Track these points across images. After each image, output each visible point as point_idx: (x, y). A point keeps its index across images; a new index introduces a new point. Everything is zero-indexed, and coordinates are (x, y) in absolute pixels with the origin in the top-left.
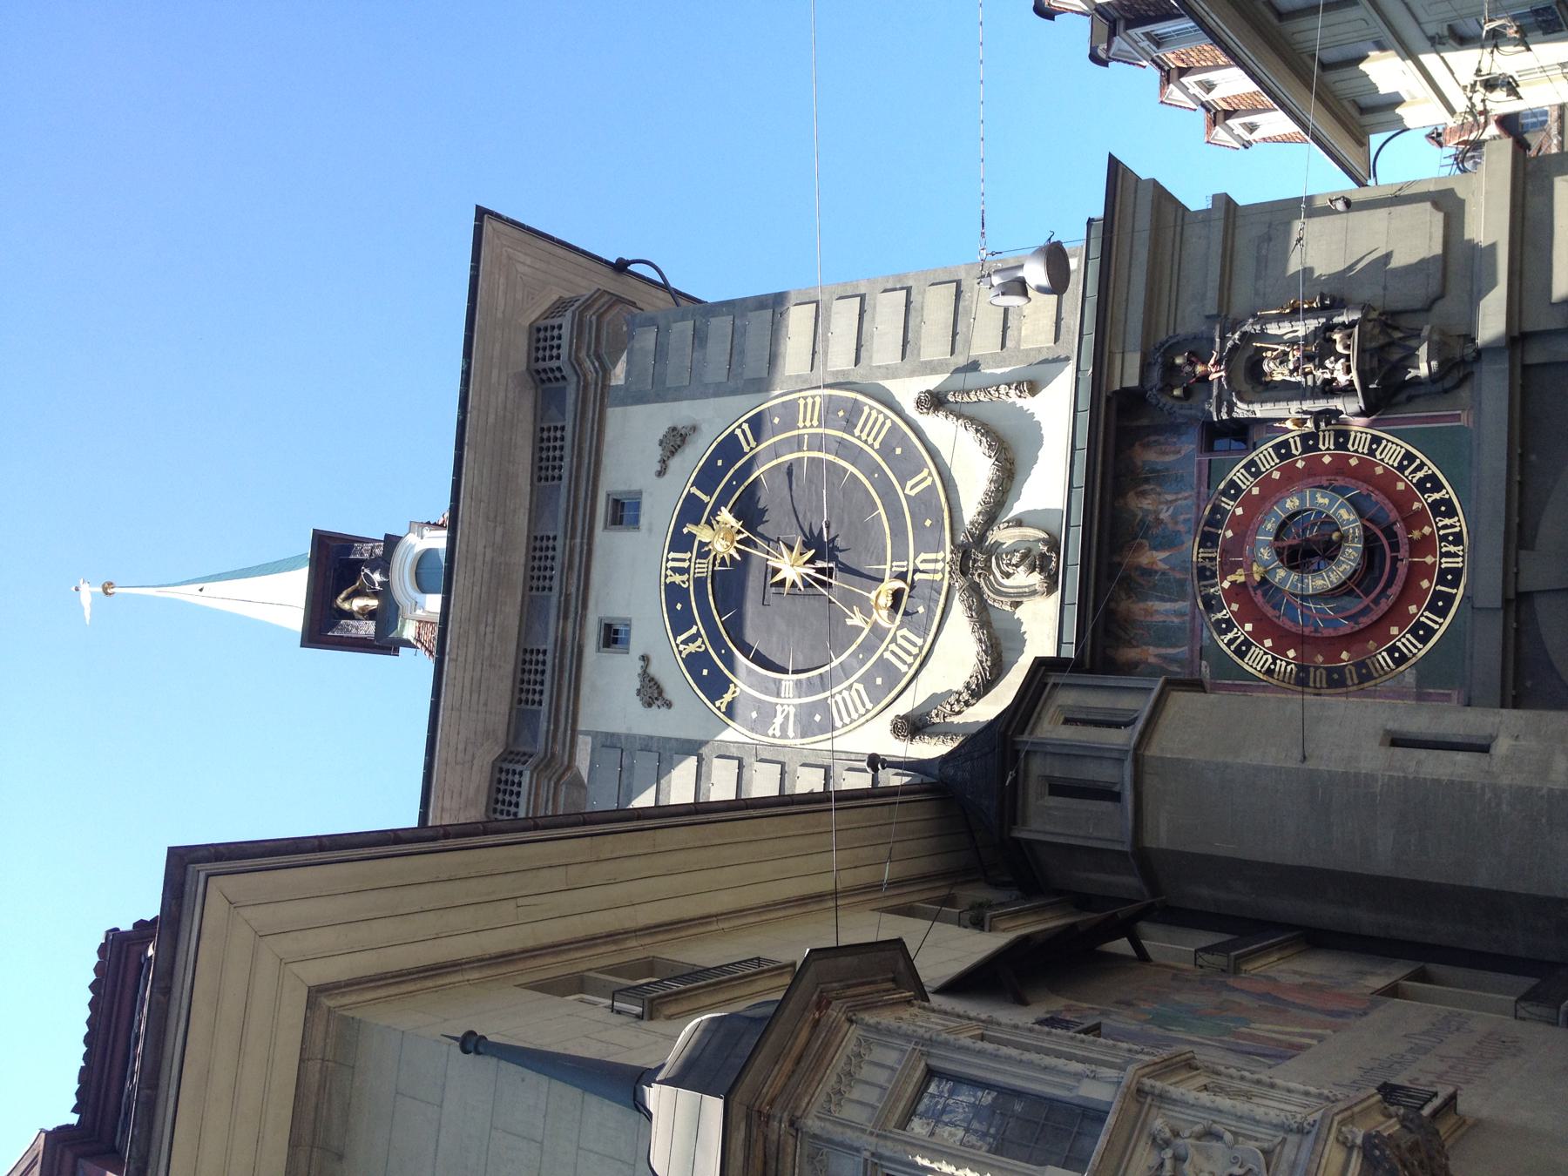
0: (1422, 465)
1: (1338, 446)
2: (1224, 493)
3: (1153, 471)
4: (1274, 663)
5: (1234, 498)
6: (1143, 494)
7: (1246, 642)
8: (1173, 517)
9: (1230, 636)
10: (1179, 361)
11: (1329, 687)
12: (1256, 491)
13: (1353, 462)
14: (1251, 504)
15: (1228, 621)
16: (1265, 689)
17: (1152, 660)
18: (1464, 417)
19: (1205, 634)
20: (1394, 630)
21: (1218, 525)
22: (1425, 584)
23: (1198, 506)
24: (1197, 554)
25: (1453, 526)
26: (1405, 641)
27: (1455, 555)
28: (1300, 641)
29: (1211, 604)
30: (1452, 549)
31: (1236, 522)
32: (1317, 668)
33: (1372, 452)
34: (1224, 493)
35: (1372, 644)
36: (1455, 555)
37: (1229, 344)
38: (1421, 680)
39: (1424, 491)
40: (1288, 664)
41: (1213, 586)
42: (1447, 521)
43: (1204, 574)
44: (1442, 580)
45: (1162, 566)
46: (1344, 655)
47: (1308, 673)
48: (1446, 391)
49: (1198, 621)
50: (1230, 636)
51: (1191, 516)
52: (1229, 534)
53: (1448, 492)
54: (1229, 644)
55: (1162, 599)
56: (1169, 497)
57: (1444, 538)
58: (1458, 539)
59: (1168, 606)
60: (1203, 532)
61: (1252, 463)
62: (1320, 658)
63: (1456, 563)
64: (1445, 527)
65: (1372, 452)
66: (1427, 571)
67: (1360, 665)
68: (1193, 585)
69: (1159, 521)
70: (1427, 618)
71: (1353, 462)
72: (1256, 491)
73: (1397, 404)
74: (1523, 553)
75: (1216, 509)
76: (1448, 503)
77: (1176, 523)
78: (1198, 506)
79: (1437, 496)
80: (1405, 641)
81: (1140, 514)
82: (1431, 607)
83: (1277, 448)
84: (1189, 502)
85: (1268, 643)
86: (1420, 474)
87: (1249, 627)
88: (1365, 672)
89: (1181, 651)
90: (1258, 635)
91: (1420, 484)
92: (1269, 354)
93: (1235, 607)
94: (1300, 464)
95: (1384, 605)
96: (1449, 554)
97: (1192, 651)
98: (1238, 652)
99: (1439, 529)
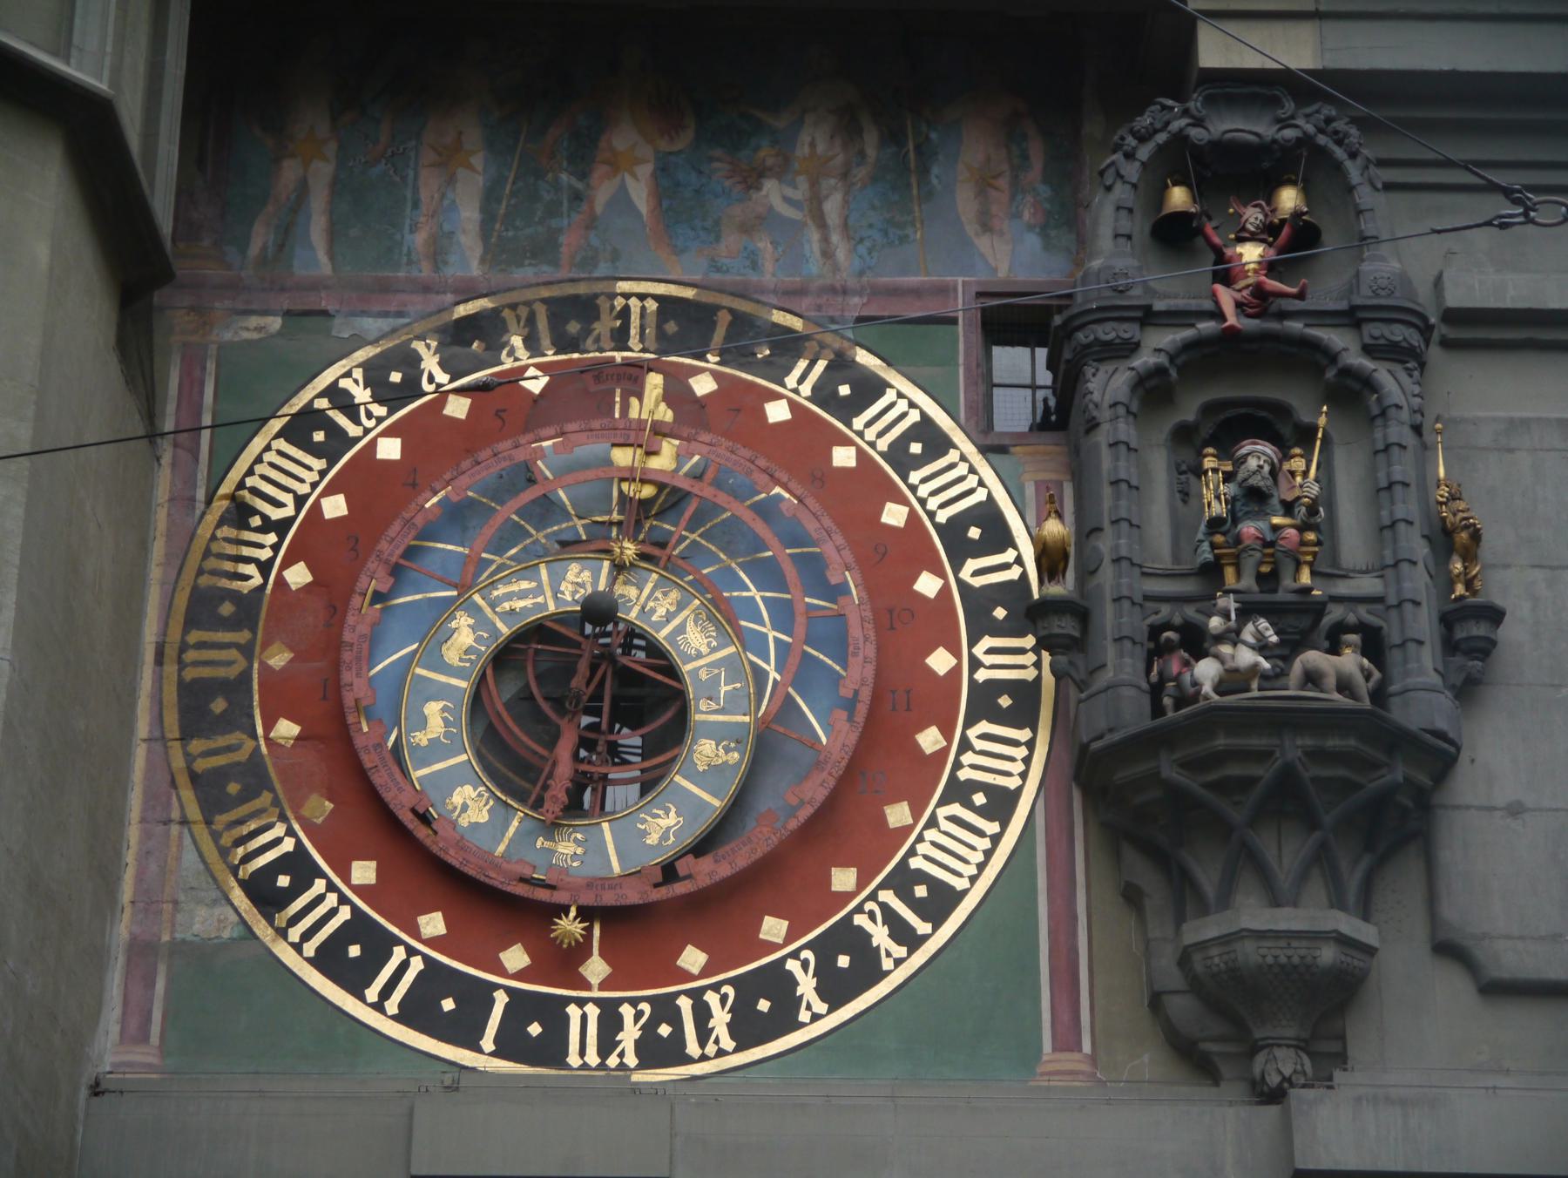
0: (912, 941)
1: (984, 702)
2: (841, 366)
3: (925, 155)
4: (268, 526)
5: (823, 394)
6: (849, 128)
7: (339, 440)
8: (765, 220)
9: (362, 395)
10: (1289, 199)
11: (184, 688)
12: (843, 457)
13: (929, 739)
14: (804, 442)
15: (411, 389)
17: (290, 172)
18: (1069, 1061)
19: (371, 325)
20: (364, 872)
21: (735, 354)
22: (515, 958)
23: (801, 292)
24: (638, 293)
25: (704, 1035)
26: (328, 904)
27: (607, 1044)
29: (465, 338)
30: (630, 1034)
31: (738, 406)
32: (247, 650)
33: (959, 792)
34: (841, 366)
35: (321, 808)
36: (607, 1044)
37: (1336, 338)
38: (197, 958)
39: (825, 949)
40: (264, 568)
41: (532, 345)
42: (720, 1019)
43: (572, 317)
44: (522, 1008)
45: (602, 194)
46: (287, 729)
47: (232, 624)
48: (1156, 1002)
49: (416, 304)
50: (362, 395)
51: (770, 274)
52: (703, 385)
53: (818, 1020)
54: (332, 392)
55: (489, 199)
56: (832, 207)
58: (655, 1051)
59: (469, 214)
60: (713, 309)
61: (937, 444)
62: (279, 659)
63: (581, 1051)
64: (702, 1014)
66: (562, 963)
67: (254, 776)
68: (534, 281)
69: (752, 178)
70: (404, 966)
72: (843, 457)
73: (1117, 856)
75: (788, 347)
76: (785, 1020)
77: (746, 229)
78: (801, 292)
79: (806, 985)
80: (328, 904)
81: (781, 123)
82: (434, 976)
83: (987, 514)
84: (814, 266)
85: (335, 507)
86: (880, 935)
88: (224, 793)
89: (316, 256)
90: (363, 479)
93: (458, 408)
94: (927, 585)
96: (610, 1024)
97: (315, 286)
99: (696, 995)
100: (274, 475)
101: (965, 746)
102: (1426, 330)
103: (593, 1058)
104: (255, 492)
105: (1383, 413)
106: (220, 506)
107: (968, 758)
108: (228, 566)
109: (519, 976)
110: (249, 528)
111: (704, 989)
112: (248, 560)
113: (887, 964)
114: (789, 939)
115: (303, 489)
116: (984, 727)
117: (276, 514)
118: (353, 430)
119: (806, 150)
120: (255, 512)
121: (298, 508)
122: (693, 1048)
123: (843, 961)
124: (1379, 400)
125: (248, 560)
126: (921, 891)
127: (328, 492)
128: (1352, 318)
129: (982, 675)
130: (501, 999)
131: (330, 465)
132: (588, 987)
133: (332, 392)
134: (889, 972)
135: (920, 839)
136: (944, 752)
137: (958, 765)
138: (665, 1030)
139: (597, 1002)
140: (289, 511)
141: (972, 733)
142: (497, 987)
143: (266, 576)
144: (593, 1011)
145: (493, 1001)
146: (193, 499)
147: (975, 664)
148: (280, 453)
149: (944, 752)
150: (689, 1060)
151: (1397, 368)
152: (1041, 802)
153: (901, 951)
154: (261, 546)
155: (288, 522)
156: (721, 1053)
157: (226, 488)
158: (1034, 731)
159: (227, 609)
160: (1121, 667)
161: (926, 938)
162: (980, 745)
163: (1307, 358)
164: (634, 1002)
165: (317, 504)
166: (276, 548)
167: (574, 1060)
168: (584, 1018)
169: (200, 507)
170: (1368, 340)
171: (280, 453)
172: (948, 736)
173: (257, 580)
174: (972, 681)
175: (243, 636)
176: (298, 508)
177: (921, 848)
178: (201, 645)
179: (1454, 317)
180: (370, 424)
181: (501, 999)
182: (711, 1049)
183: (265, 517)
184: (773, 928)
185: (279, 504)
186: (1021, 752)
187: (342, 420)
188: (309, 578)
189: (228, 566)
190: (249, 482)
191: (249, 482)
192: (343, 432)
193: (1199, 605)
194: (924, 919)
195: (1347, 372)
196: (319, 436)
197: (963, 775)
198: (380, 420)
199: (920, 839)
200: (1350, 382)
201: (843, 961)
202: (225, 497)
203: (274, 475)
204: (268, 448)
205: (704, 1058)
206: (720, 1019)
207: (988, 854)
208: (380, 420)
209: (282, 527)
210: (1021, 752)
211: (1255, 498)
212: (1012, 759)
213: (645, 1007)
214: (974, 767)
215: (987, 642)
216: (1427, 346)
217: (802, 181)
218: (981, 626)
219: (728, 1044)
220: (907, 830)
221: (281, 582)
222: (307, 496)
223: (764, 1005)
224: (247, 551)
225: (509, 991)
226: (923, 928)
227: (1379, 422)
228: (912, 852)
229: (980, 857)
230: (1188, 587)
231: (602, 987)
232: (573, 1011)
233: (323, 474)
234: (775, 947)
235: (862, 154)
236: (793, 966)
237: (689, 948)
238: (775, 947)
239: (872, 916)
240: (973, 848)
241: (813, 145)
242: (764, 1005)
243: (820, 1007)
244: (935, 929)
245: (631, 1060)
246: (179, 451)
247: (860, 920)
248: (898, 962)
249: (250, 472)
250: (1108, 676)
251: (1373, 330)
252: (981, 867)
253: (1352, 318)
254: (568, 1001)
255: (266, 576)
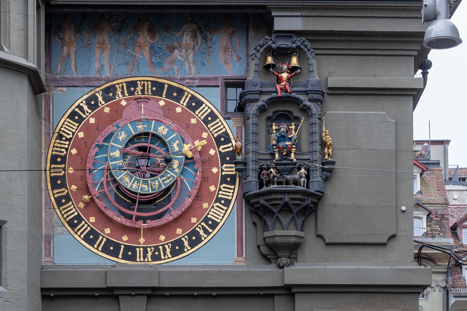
1: (224, 180)
4: (67, 140)
7: (81, 119)
16: (48, 134)
27: (145, 257)
28: (83, 156)
30: (149, 254)
33: (218, 200)
36: (145, 257)
37: (302, 97)
40: (67, 149)
42: (168, 251)
44: (127, 248)
57: (157, 249)
58: (156, 258)
64: (164, 250)
65: (218, 200)
71: (212, 188)
74: (146, 297)
79: (186, 243)
85: (81, 135)
86: (201, 232)
87: (92, 121)
90: (87, 128)
91: (194, 232)
92: (293, 127)
95: (110, 213)
96: (145, 252)
98: (74, 114)
99: (163, 246)
100: (67, 127)
101: (220, 190)
102: (323, 94)
103: (142, 260)
104: (63, 131)
105: (312, 115)
106: (56, 135)
107: (220, 192)
108: (59, 149)
109: (126, 242)
110: (62, 140)
111: (164, 244)
112: (63, 148)
113: (203, 238)
114: (182, 233)
115: (74, 131)
116: (224, 185)
117: (68, 137)
118: (84, 116)
119: (185, 42)
120: (64, 136)
121: (73, 136)
122: (163, 257)
123: (194, 238)
124: (311, 112)
125: (63, 148)
126: (210, 222)
127: (79, 131)
128: (306, 93)
129: (224, 173)
130: (123, 247)
131: (80, 124)
132: (141, 244)
133: (79, 107)
134: (203, 240)
135: (210, 211)
136: (215, 191)
137: (218, 194)
138: (157, 253)
139: (142, 247)
140: (71, 136)
141: (221, 187)
142: (122, 244)
143: (67, 152)
144: (142, 249)
145: (121, 247)
146: (50, 133)
147: (222, 171)
148: (68, 122)
149: (216, 191)
150: (162, 260)
151: (316, 104)
152: (236, 202)
153: (206, 236)
154: (66, 145)
155: (71, 138)
156: (169, 258)
157: (57, 131)
158: (235, 186)
159: (59, 160)
160: (252, 177)
161: (211, 233)
162: (223, 189)
163: (296, 102)
164: (150, 247)
165: (77, 134)
166: (69, 145)
167: (138, 260)
168: (140, 251)
169: (52, 135)
170: (310, 98)
171: (68, 122)
172: (216, 187)
173: (65, 152)
174: (221, 174)
175: (63, 166)
176: (73, 136)
177: (210, 213)
178: (54, 168)
179: (330, 89)
180: (88, 114)
181: (123, 247)
182: (166, 257)
183: (66, 138)
184: (179, 231)
185: (69, 134)
186: (232, 191)
187: (82, 114)
188: (76, 152)
189: (59, 149)
190: (62, 129)
191: (62, 129)
192: (82, 116)
193: (270, 161)
194: (211, 229)
195: (304, 105)
196: (76, 118)
197: (219, 196)
198: (90, 113)
199: (210, 211)
200: (305, 108)
201: (194, 238)
202: (57, 133)
203: (67, 127)
204: (65, 121)
205: (165, 259)
206: (168, 251)
207: (225, 214)
208: (90, 113)
209: (69, 140)
210: (232, 191)
211: (282, 138)
212: (230, 193)
213: (152, 248)
214: (222, 194)
215: (225, 165)
216: (323, 96)
217: (184, 51)
218: (224, 161)
219: (170, 256)
220: (208, 209)
221: (71, 153)
222: (75, 132)
223: (177, 248)
224: (62, 146)
225: (124, 245)
226: (211, 231)
227: (311, 117)
228: (208, 214)
229: (222, 215)
230: (268, 157)
231: (143, 244)
232: (138, 249)
233: (78, 127)
234: (179, 235)
235: (197, 43)
236: (183, 239)
237: (161, 235)
238: (179, 235)
239: (200, 228)
240: (221, 213)
241: (186, 41)
242: (177, 248)
243: (189, 248)
244: (213, 231)
245: (150, 260)
246: (46, 122)
247: (197, 229)
248: (205, 238)
249: (62, 127)
250: (249, 179)
251: (310, 96)
252: (223, 217)
253: (306, 93)
254: (137, 247)
255: (67, 152)
